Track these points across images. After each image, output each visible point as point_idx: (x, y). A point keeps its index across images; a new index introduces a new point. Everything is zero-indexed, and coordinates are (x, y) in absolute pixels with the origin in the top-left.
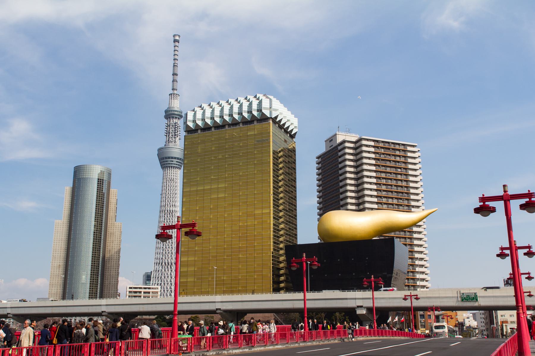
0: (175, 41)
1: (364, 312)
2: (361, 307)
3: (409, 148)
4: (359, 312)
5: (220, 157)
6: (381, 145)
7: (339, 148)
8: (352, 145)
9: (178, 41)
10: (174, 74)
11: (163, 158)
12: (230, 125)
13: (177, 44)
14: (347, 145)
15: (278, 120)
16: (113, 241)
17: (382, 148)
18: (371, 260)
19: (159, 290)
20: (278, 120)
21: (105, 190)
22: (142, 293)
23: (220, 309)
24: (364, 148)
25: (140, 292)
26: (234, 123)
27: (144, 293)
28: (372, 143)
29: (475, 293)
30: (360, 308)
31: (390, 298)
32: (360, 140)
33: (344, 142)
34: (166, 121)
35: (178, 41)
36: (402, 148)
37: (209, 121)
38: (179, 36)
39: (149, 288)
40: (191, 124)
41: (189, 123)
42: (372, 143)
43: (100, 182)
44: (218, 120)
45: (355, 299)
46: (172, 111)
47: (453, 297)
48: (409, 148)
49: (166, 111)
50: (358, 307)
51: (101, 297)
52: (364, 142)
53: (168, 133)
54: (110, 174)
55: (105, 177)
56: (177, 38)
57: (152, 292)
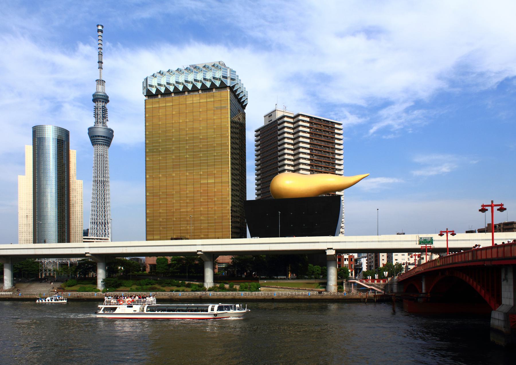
1: (333, 252)
2: (331, 249)
3: (336, 126)
4: (329, 253)
6: (314, 121)
7: (279, 122)
8: (291, 120)
14: (286, 119)
15: (237, 93)
17: (315, 124)
18: (322, 212)
20: (237, 93)
23: (201, 251)
24: (301, 123)
28: (308, 119)
29: (431, 238)
30: (330, 250)
31: (357, 242)
32: (299, 115)
33: (284, 117)
36: (330, 125)
42: (308, 119)
45: (327, 242)
47: (412, 241)
48: (336, 126)
50: (328, 249)
51: (69, 241)
52: (301, 118)
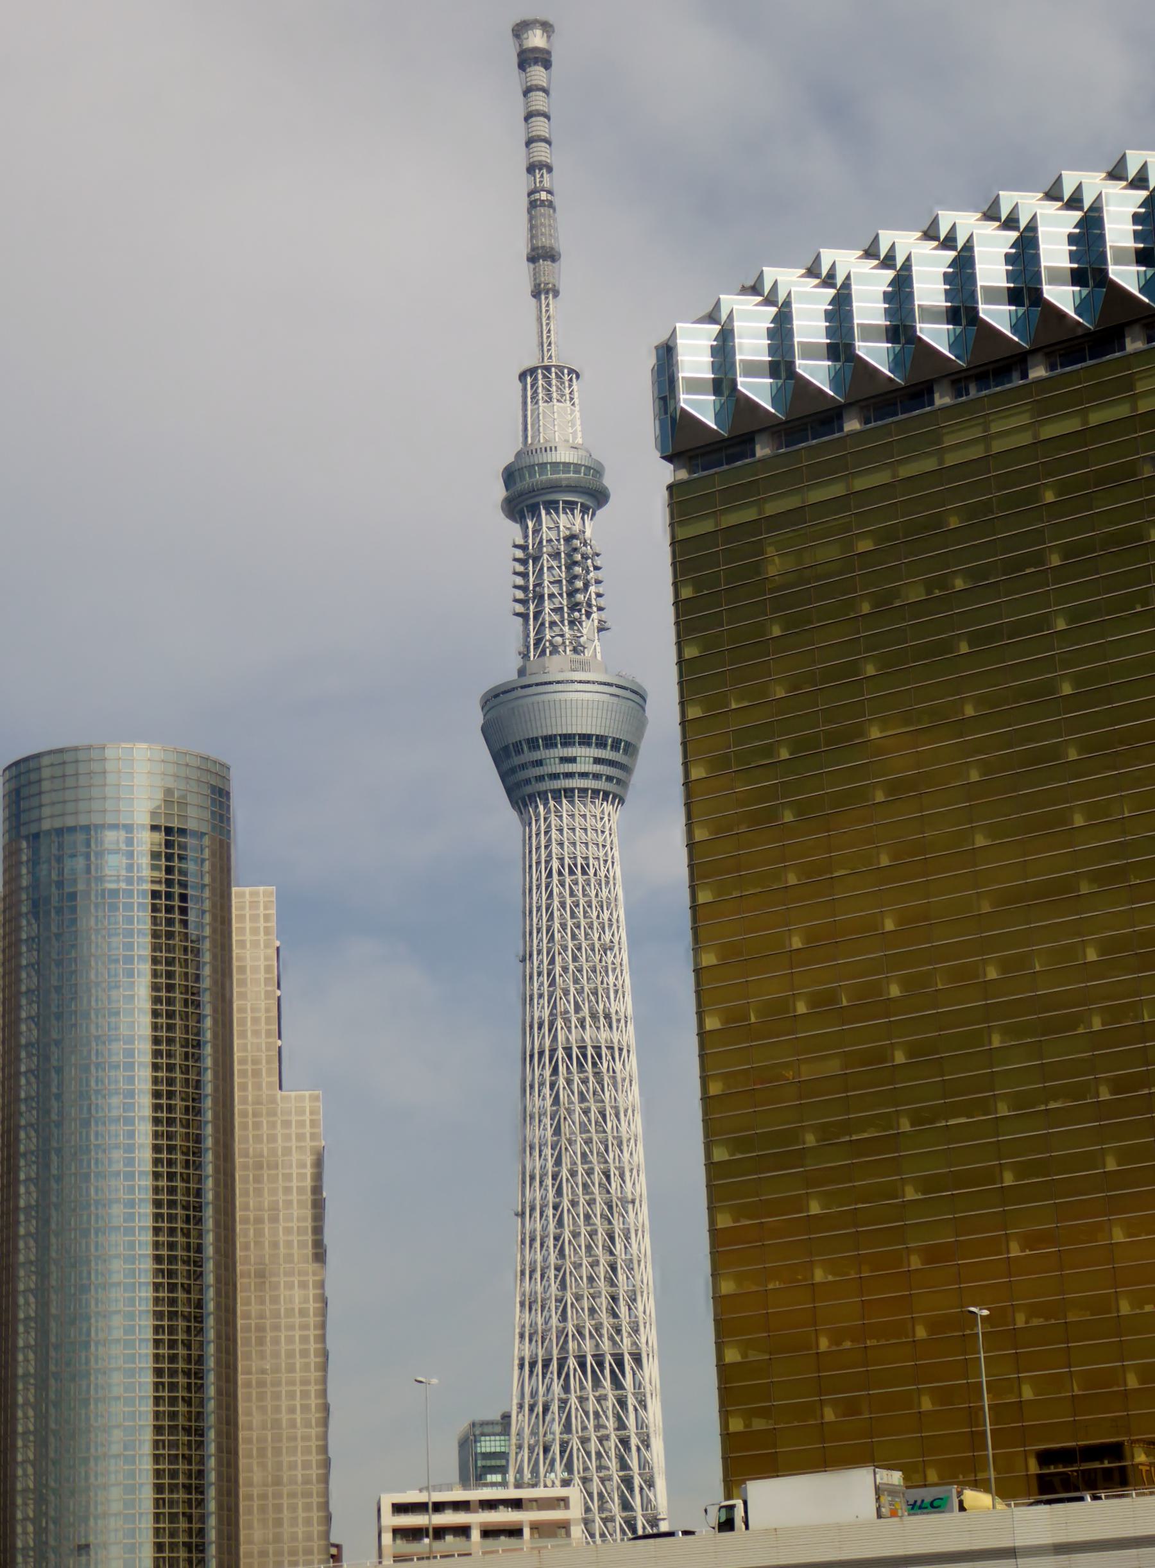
0: (527, 59)
5: (916, 595)
9: (543, 59)
10: (541, 255)
11: (518, 748)
12: (958, 380)
13: (538, 74)
16: (274, 1207)
19: (575, 1512)
21: (197, 870)
22: (475, 1534)
25: (463, 1531)
26: (990, 365)
27: (488, 1533)
34: (513, 531)
35: (543, 59)
37: (816, 372)
38: (546, 27)
39: (517, 1504)
40: (702, 407)
41: (686, 401)
43: (172, 840)
44: (875, 353)
46: (543, 466)
49: (510, 476)
53: (530, 598)
54: (220, 796)
55: (192, 812)
56: (536, 39)
57: (536, 1527)
